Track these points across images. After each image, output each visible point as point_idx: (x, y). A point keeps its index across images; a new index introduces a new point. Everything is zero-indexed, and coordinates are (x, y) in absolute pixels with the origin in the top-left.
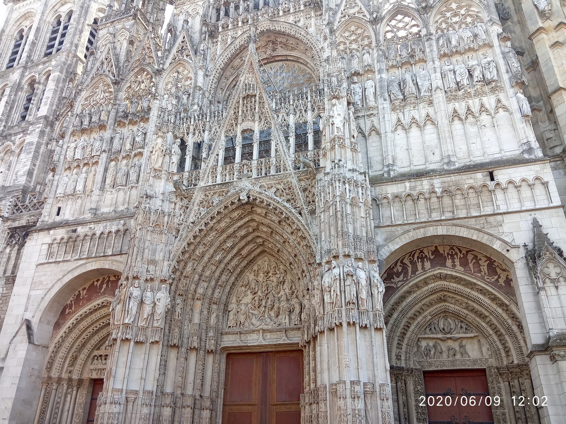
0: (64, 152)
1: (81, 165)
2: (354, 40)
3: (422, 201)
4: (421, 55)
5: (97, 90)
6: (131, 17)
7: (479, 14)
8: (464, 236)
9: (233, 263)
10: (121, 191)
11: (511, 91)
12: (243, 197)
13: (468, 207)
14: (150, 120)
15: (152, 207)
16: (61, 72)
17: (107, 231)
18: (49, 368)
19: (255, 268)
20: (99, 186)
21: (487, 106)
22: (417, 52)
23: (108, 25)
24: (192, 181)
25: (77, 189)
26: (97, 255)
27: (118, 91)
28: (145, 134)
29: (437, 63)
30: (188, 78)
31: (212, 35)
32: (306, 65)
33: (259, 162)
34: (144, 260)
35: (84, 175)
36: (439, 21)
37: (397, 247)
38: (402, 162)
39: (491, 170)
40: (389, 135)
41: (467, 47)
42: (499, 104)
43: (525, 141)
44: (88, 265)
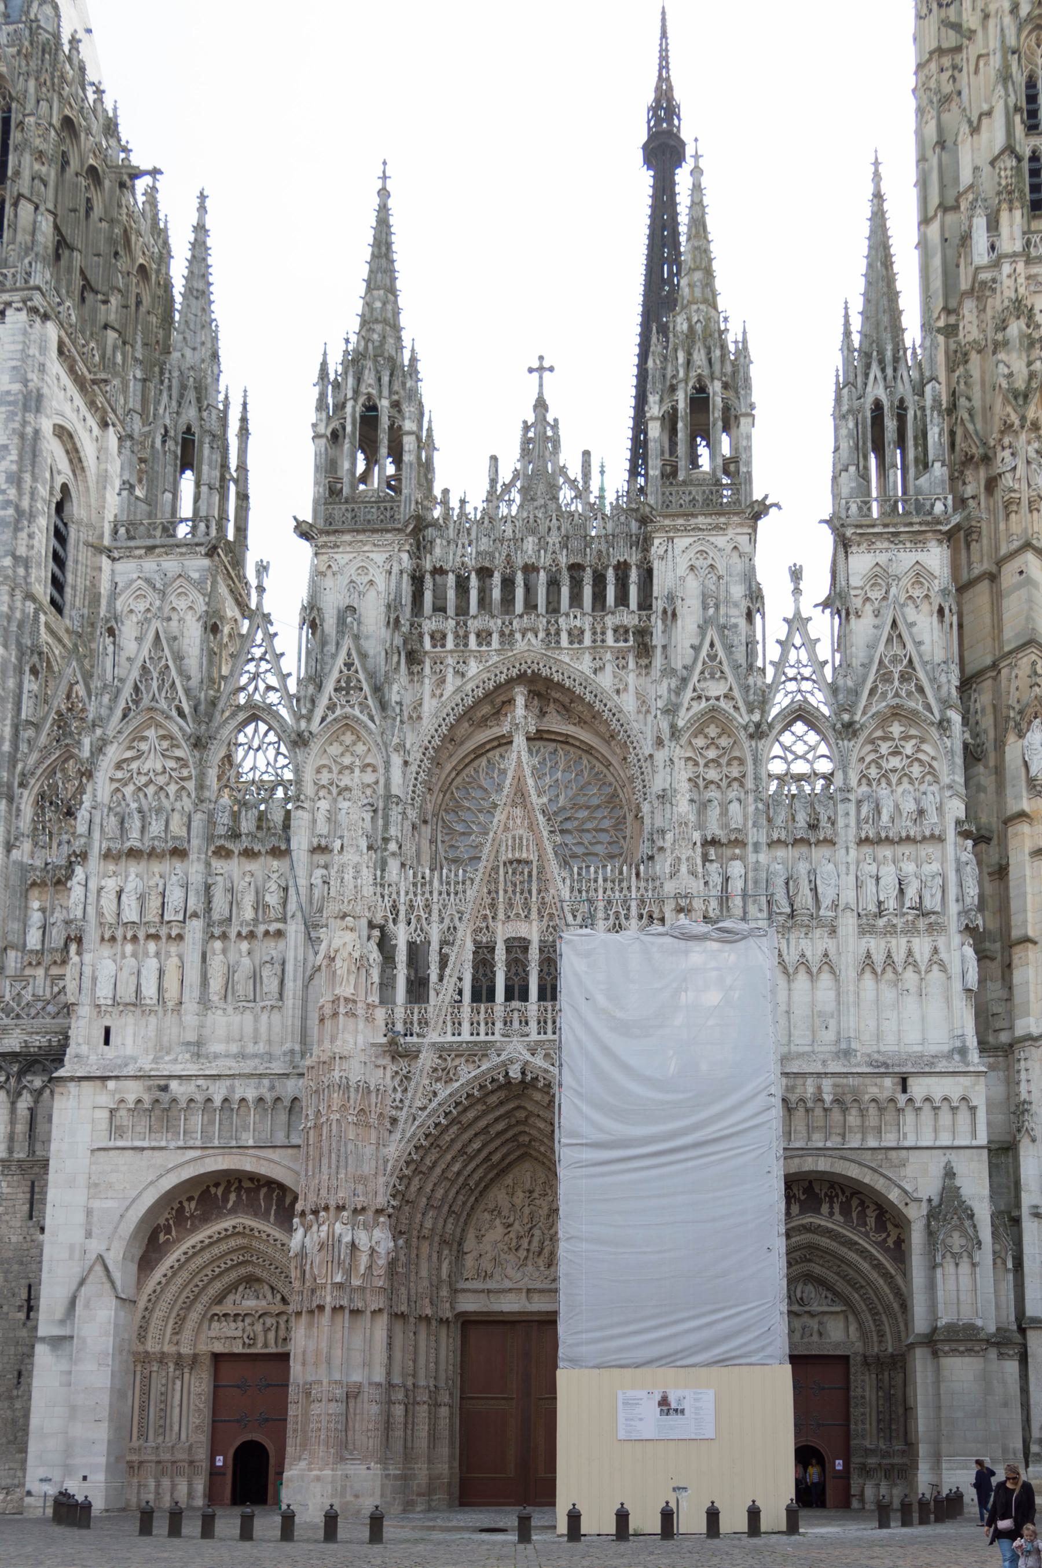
0: (92, 898)
1: (141, 935)
2: (713, 760)
3: (800, 1113)
4: (829, 832)
5: (144, 746)
7: (935, 764)
10: (248, 1012)
11: (956, 939)
12: (515, 1073)
13: (863, 1130)
17: (237, 1097)
18: (142, 1337)
20: (196, 994)
21: (917, 956)
22: (824, 823)
28: (286, 889)
29: (853, 852)
35: (152, 964)
36: (868, 759)
41: (904, 834)
42: (935, 958)
43: (960, 1033)
44: (207, 1160)
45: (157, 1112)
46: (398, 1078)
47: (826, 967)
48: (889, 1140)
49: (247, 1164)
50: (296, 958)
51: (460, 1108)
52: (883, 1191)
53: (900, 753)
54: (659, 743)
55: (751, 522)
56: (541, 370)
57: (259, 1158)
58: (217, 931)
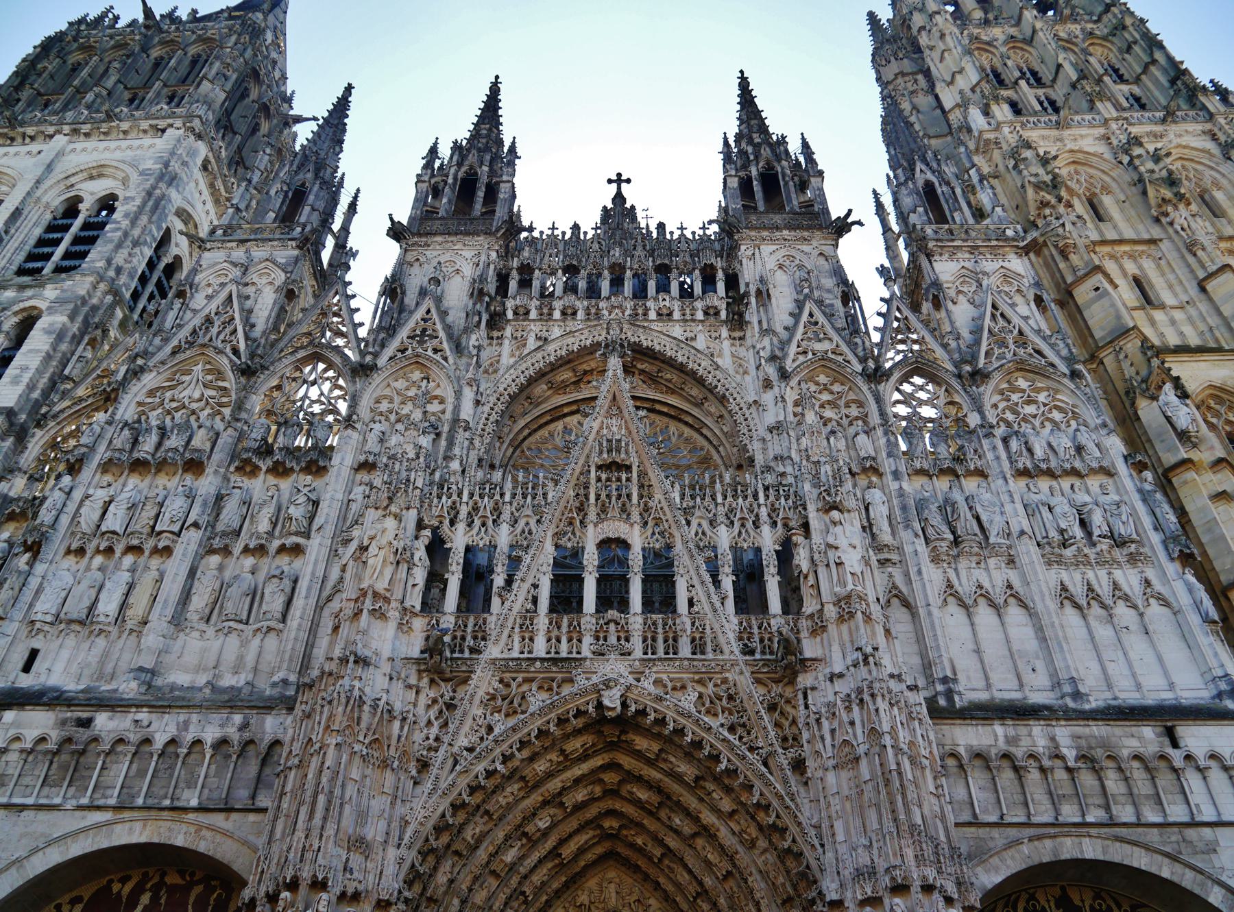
0: (71, 507)
1: (119, 549)
2: (829, 402)
3: (1034, 776)
5: (186, 378)
6: (294, 244)
8: (1143, 868)
9: (536, 879)
10: (234, 635)
11: (1172, 568)
12: (612, 700)
14: (333, 472)
15: (367, 690)
16: (72, 317)
17: (189, 737)
19: (583, 898)
20: (169, 612)
22: (970, 455)
23: (229, 245)
24: (463, 638)
25: (101, 607)
26: (150, 802)
27: (246, 390)
28: (316, 504)
30: (436, 397)
31: (496, 321)
32: (698, 431)
33: (649, 622)
34: (341, 835)
37: (998, 879)
38: (968, 678)
39: (1169, 724)
40: (935, 612)
42: (1149, 590)
43: (1220, 673)
44: (118, 828)
45: (64, 757)
46: (436, 707)
47: (1012, 600)
48: (1177, 813)
49: (179, 835)
50: (313, 574)
51: (526, 753)
52: (1197, 891)
53: (1035, 402)
54: (768, 384)
55: (834, 236)
56: (619, 180)
57: (200, 827)
58: (217, 543)
